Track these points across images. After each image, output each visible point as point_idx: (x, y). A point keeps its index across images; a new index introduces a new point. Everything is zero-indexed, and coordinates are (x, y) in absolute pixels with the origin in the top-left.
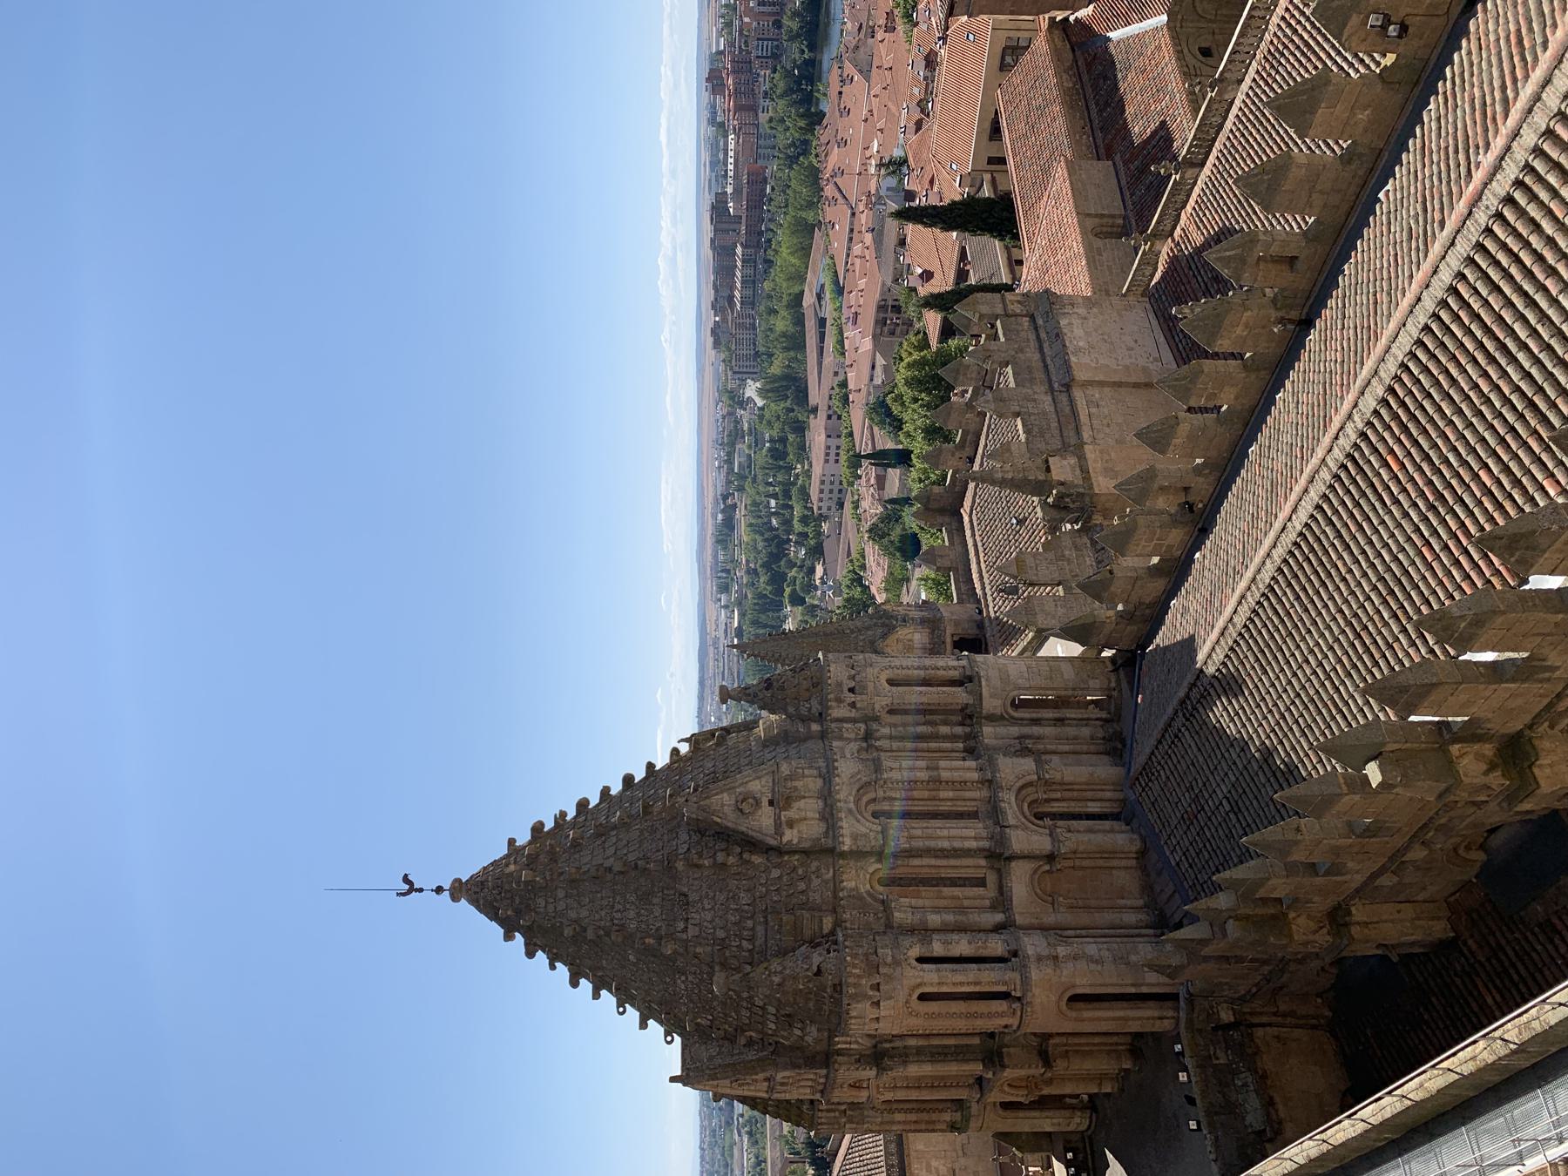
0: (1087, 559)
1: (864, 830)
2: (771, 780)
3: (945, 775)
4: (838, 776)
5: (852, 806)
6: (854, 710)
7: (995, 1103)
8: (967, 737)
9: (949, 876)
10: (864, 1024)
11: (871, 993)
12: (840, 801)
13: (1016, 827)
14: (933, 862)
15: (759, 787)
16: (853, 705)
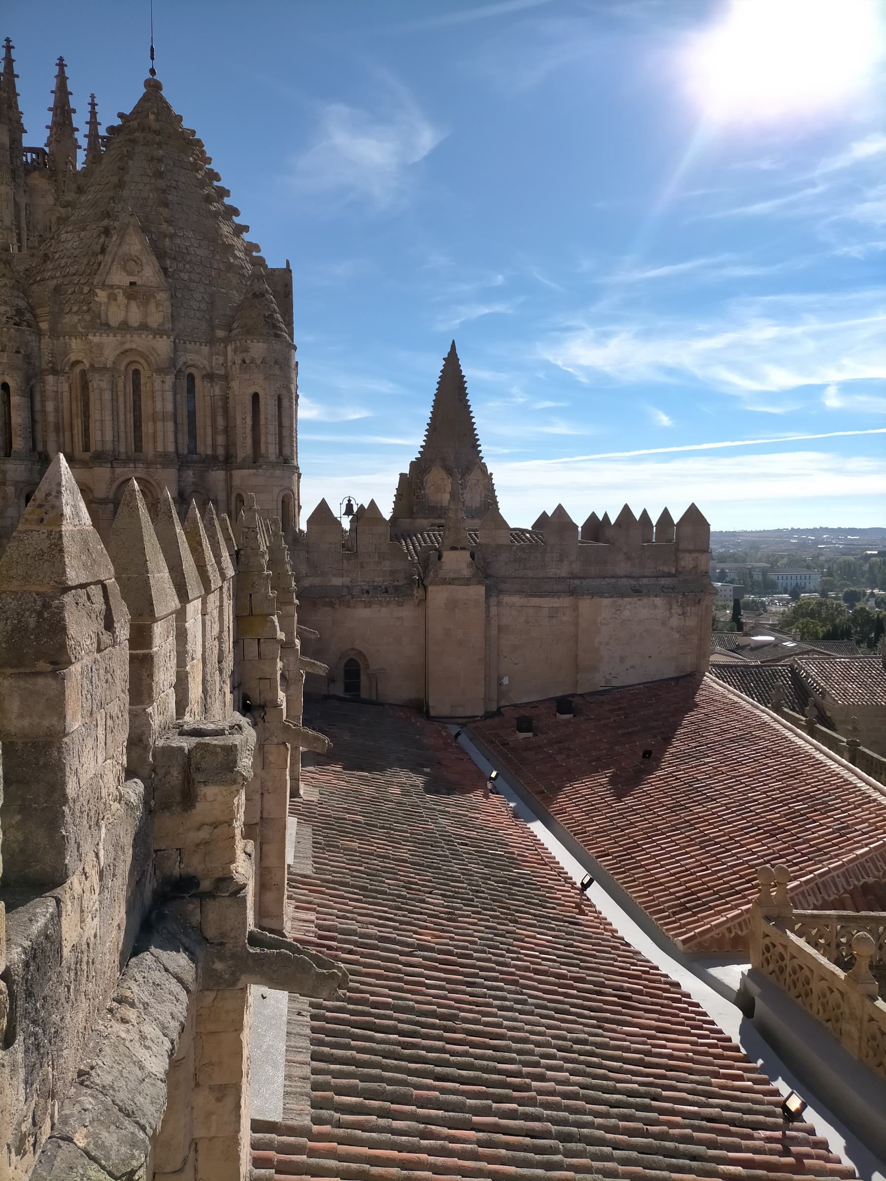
0: (381, 579)
1: (106, 353)
2: (153, 284)
3: (159, 424)
4: (154, 337)
5: (127, 346)
8: (215, 457)
12: (132, 336)
13: (113, 473)
15: (147, 275)
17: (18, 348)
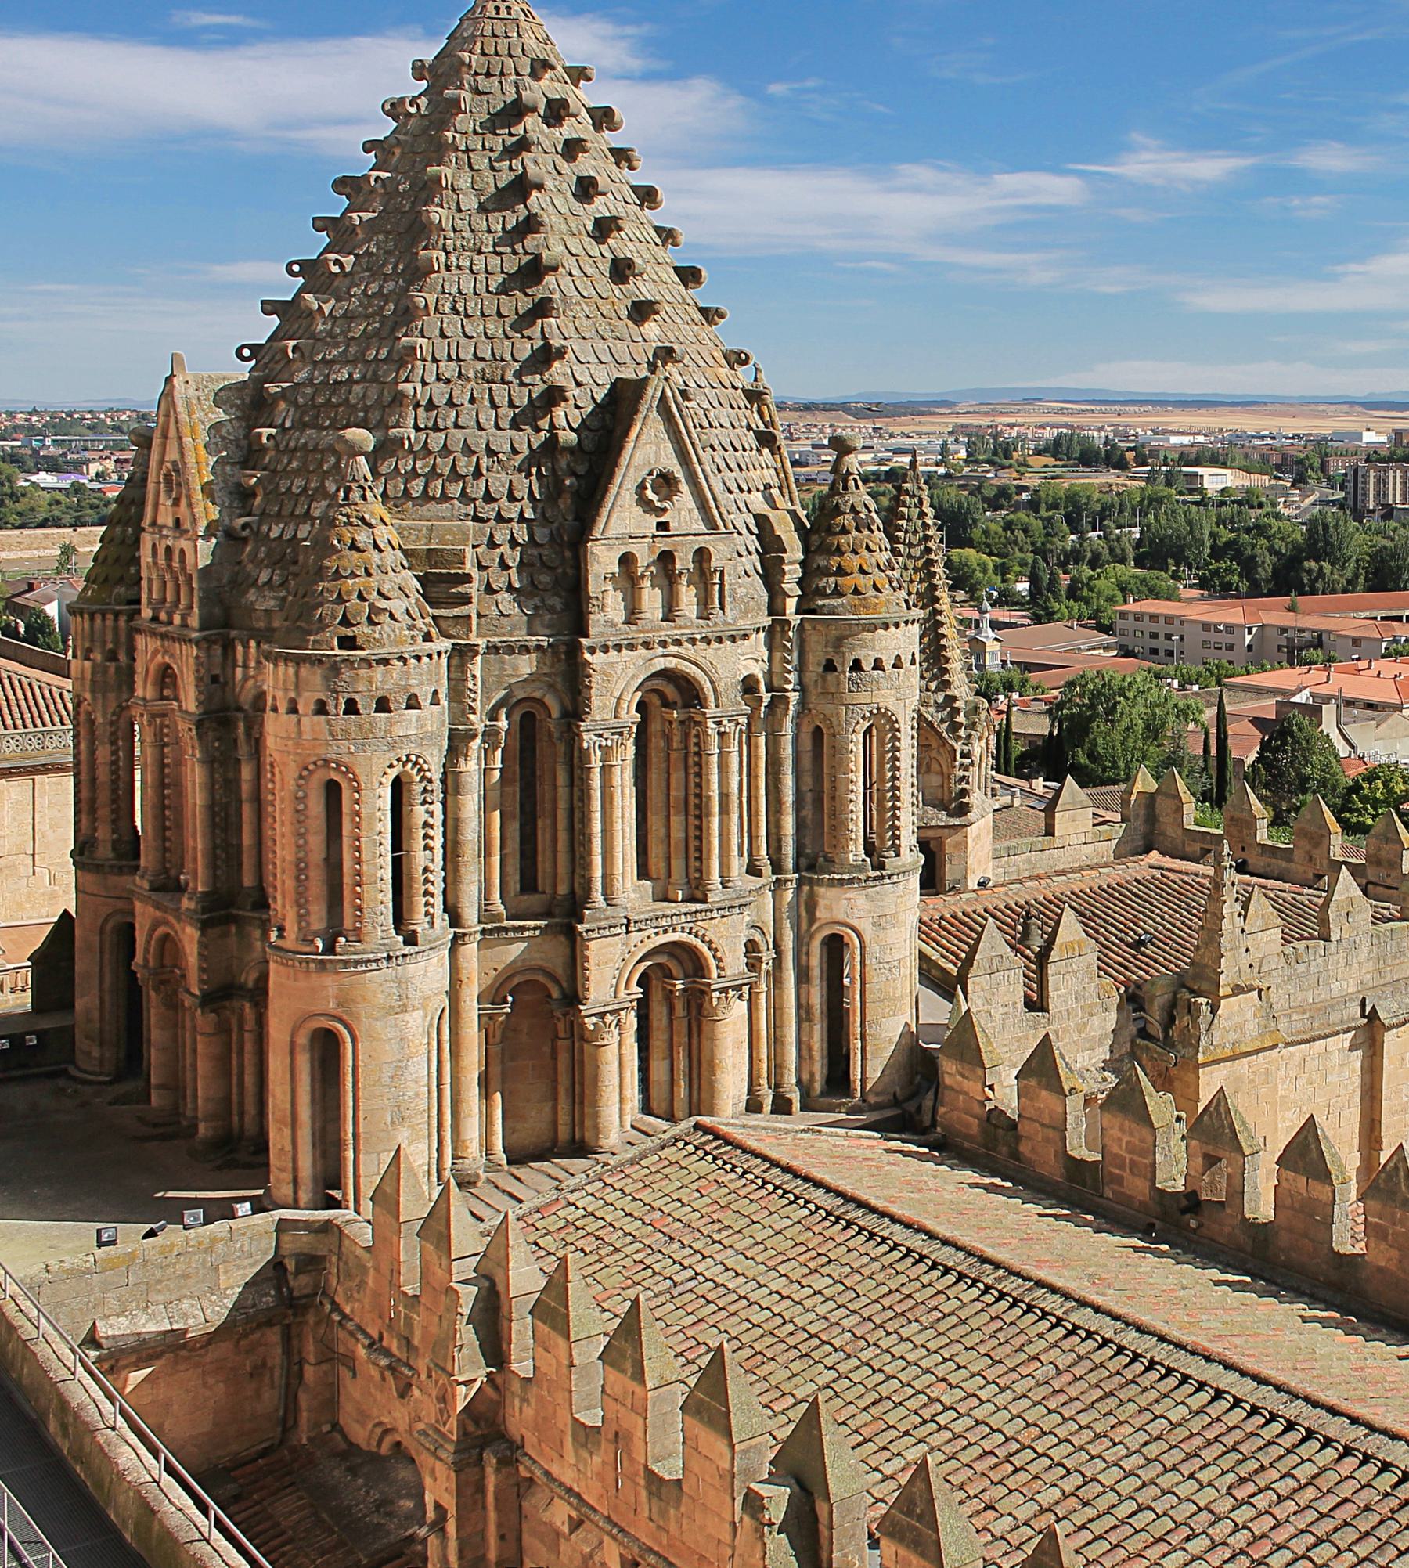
6: (821, 669)
7: (132, 913)
9: (539, 833)
10: (286, 690)
11: (342, 701)
14: (562, 805)
16: (830, 667)
17: (435, 692)
